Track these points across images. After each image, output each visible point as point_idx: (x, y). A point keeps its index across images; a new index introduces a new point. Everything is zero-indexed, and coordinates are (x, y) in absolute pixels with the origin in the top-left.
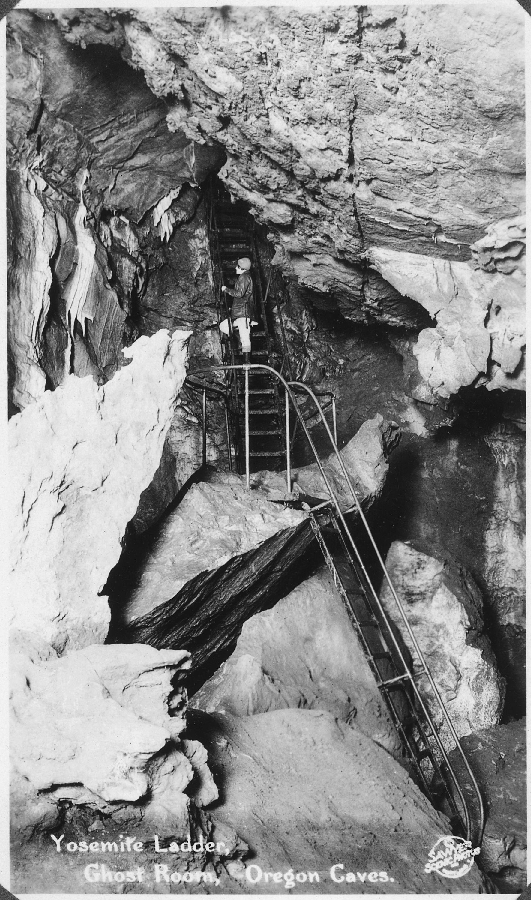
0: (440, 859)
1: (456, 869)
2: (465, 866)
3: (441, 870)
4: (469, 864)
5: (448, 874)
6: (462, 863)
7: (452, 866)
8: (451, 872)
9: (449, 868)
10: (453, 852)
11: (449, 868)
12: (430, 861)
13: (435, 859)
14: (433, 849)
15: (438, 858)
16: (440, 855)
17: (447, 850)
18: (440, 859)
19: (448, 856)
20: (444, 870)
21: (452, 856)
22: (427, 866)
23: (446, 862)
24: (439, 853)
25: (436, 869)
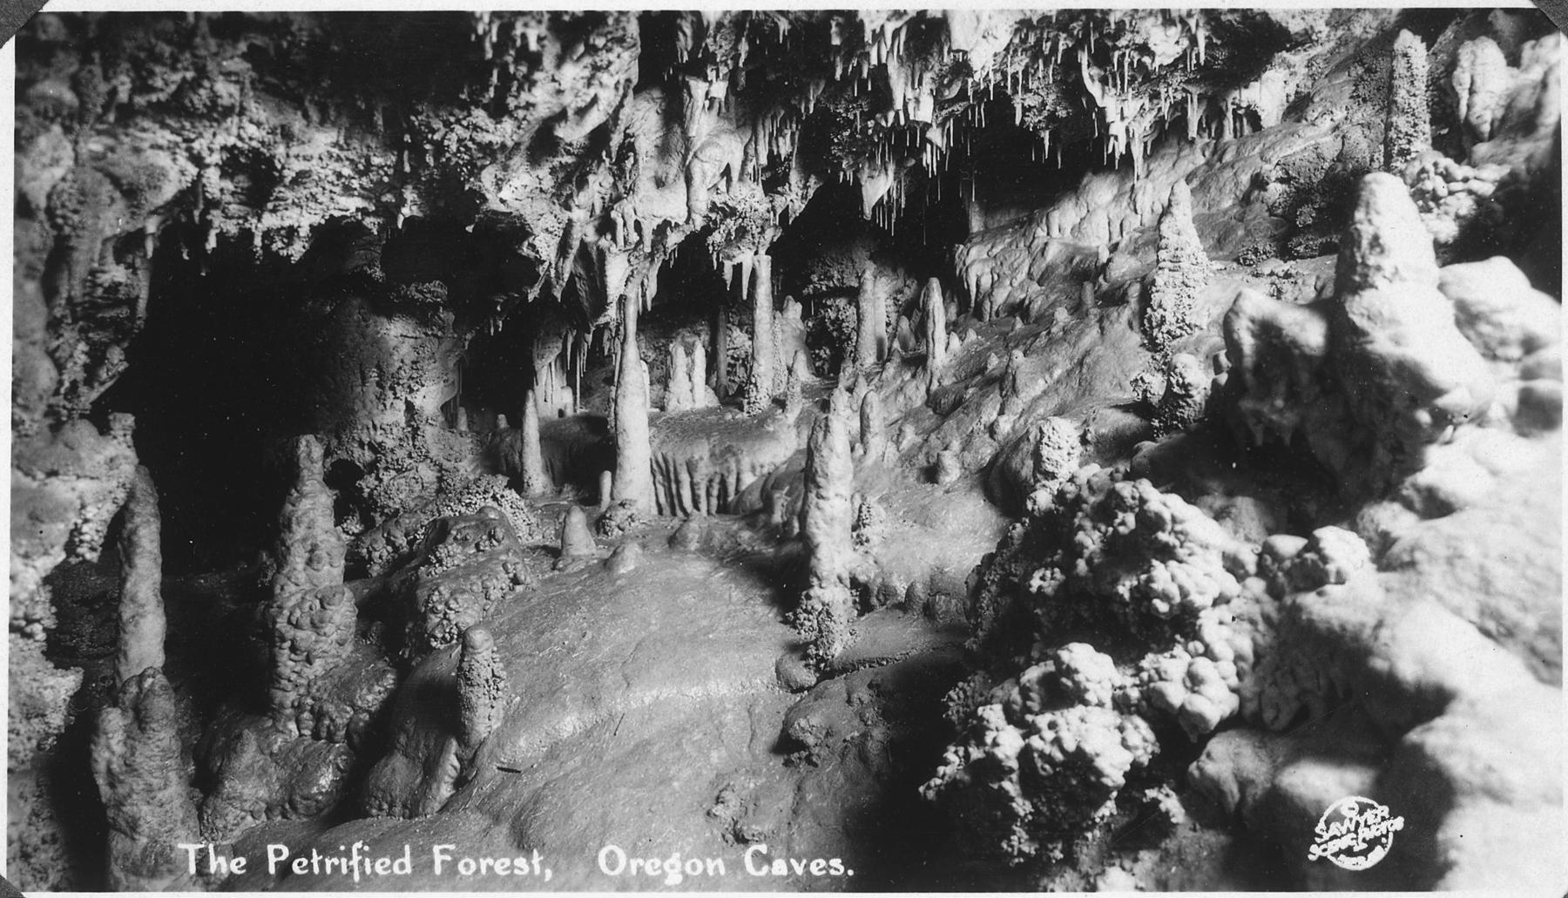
0: (1334, 837)
1: (1364, 853)
2: (1379, 848)
3: (1336, 855)
4: (1384, 846)
5: (1346, 863)
6: (1372, 844)
7: (1356, 849)
8: (1354, 860)
9: (1349, 852)
10: (1358, 824)
11: (1349, 852)
12: (1318, 840)
13: (1326, 836)
14: (1323, 820)
15: (1331, 833)
16: (1335, 828)
17: (1347, 822)
18: (1332, 838)
19: (1349, 831)
20: (1342, 857)
21: (1356, 832)
22: (1313, 848)
23: (1344, 843)
24: (1333, 826)
25: (1328, 854)
